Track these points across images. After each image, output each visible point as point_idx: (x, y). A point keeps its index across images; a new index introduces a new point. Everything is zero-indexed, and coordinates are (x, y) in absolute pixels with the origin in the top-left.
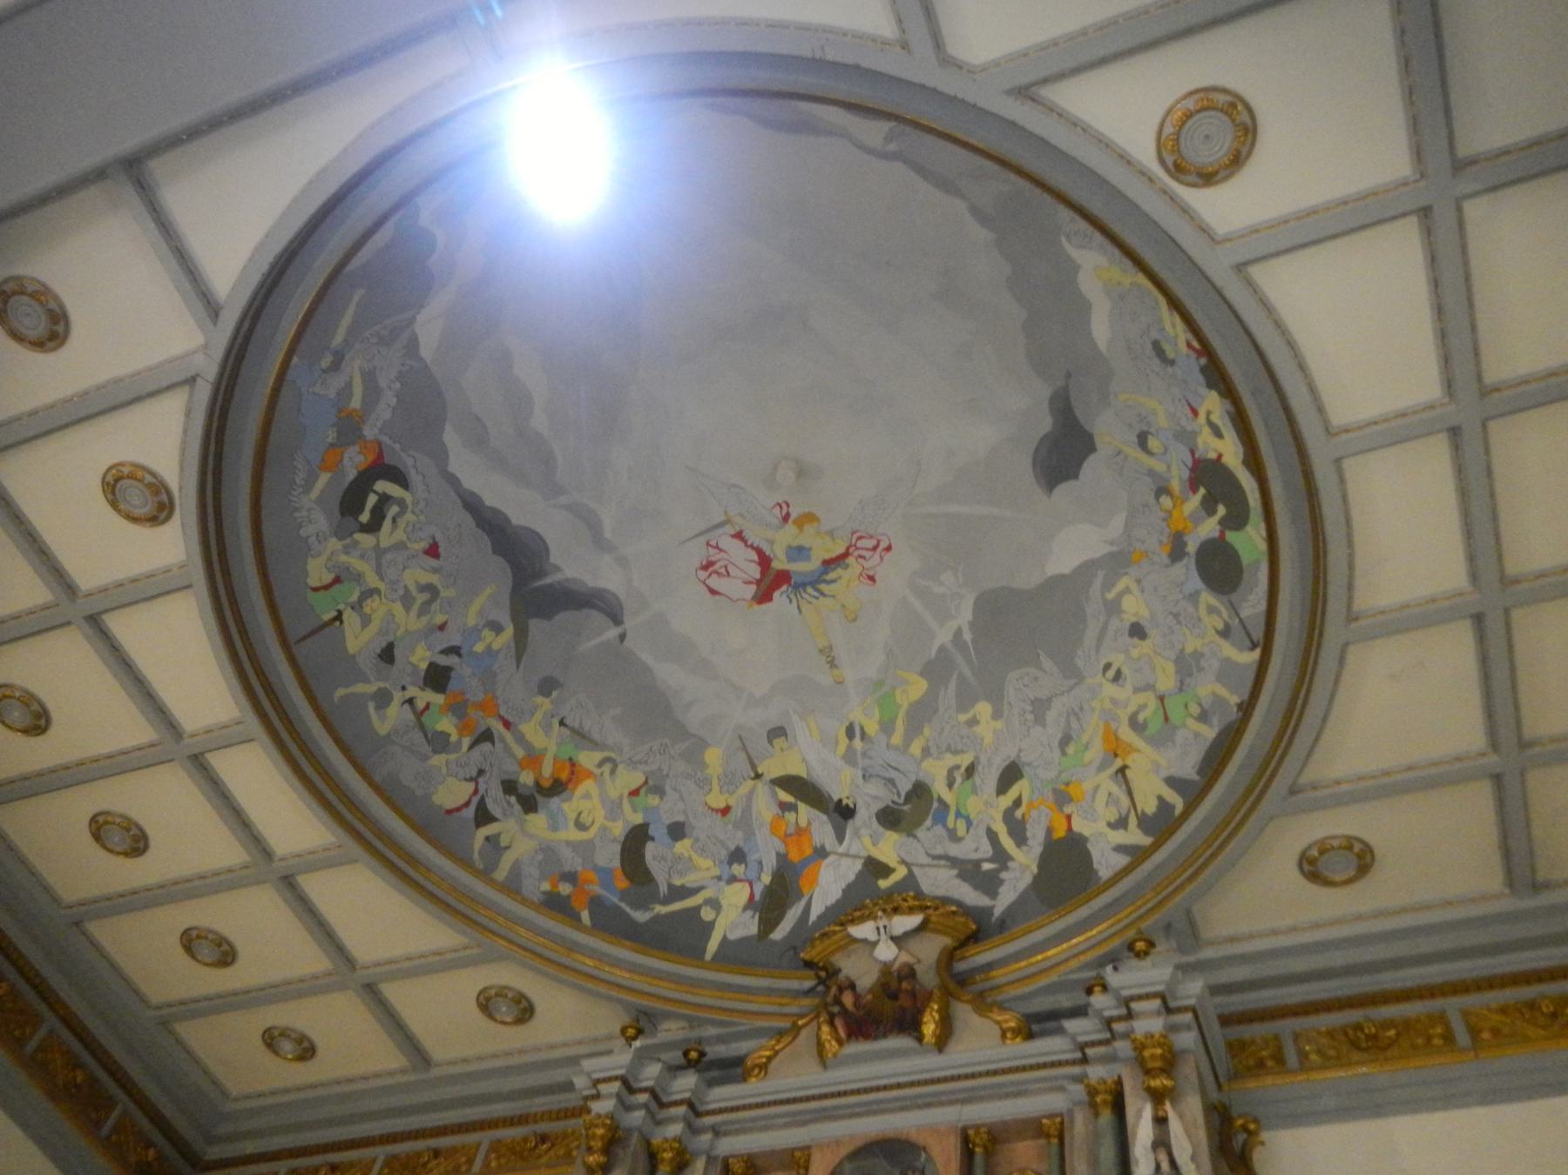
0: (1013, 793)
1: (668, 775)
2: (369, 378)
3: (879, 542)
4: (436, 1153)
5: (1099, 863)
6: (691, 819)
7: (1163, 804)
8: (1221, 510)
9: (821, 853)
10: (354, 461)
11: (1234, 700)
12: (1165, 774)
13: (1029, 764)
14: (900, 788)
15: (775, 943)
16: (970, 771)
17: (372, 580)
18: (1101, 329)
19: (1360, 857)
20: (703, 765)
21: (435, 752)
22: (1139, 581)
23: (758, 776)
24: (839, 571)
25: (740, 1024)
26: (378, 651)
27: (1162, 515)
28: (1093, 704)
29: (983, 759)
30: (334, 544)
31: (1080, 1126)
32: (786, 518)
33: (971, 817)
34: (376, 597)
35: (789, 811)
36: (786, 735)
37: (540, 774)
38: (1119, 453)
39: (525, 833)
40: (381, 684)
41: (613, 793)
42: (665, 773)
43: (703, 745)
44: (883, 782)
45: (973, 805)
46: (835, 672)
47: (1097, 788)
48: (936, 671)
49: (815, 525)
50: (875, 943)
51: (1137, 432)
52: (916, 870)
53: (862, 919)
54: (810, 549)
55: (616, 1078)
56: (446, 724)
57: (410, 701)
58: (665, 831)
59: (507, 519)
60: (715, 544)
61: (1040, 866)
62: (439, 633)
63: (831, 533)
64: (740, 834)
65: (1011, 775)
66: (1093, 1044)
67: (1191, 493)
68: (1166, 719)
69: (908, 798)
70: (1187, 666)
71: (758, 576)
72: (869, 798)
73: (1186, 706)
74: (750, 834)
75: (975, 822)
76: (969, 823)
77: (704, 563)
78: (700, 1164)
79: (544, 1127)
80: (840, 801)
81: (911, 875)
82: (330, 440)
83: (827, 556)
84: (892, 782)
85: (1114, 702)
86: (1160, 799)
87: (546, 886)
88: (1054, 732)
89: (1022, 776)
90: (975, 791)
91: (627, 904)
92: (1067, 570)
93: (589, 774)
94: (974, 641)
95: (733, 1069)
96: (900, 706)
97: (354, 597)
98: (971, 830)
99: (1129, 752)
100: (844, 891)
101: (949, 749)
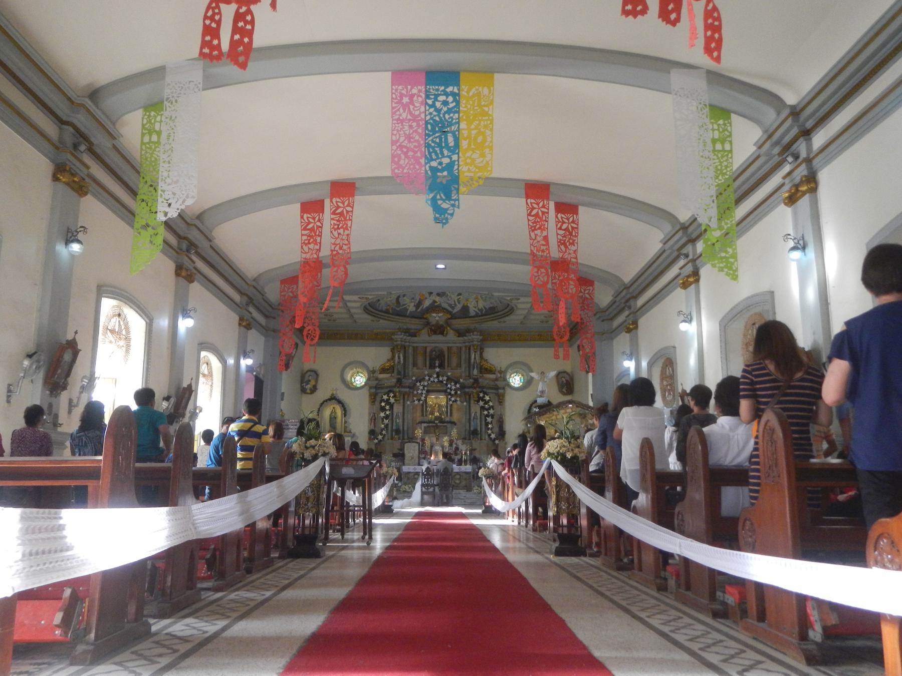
9: (426, 298)
11: (496, 305)
31: (464, 349)
45: (452, 296)
65: (459, 294)
78: (411, 348)
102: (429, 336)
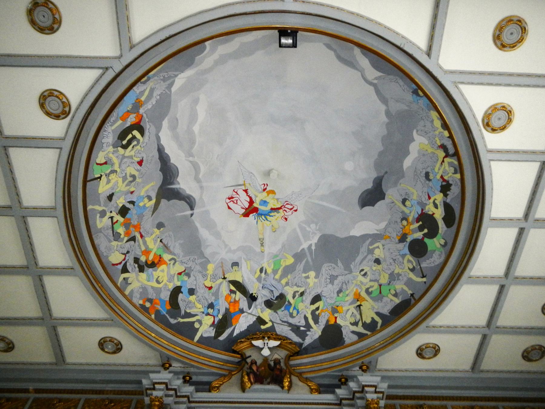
0: (316, 305)
1: (193, 270)
2: (152, 91)
3: (294, 207)
4: (60, 400)
5: (345, 336)
6: (198, 288)
7: (374, 321)
8: (426, 231)
9: (242, 311)
10: (132, 119)
11: (410, 292)
12: (375, 311)
13: (324, 297)
14: (275, 295)
15: (219, 340)
16: (302, 294)
17: (116, 167)
18: (407, 163)
19: (436, 351)
20: (207, 270)
21: (115, 240)
22: (383, 245)
23: (225, 278)
24: (275, 213)
25: (204, 369)
26: (108, 195)
27: (402, 227)
28: (353, 281)
29: (308, 291)
30: (111, 149)
32: (264, 190)
33: (299, 310)
34: (115, 174)
35: (233, 294)
36: (238, 266)
37: (148, 258)
38: (393, 203)
39: (138, 281)
40: (104, 208)
41: (172, 272)
42: (192, 269)
43: (208, 262)
44: (269, 291)
45: (301, 306)
46: (262, 248)
47: (348, 310)
48: (299, 257)
49: (274, 195)
50: (262, 349)
51: (403, 198)
52: (275, 325)
53: (257, 339)
54: (268, 203)
55: (163, 383)
56: (121, 230)
57: (112, 218)
58: (187, 290)
59: (170, 160)
60: (236, 191)
61: (322, 333)
62: (130, 194)
63: (277, 199)
64: (213, 298)
65: (317, 299)
66: (346, 399)
67: (416, 222)
68: (380, 293)
69: (277, 298)
70: (393, 277)
71: (247, 207)
72: (263, 295)
73: (390, 290)
74: (217, 299)
75: (300, 313)
76: (298, 312)
77: (230, 197)
79: (112, 396)
80: (252, 294)
81: (273, 326)
82: (128, 109)
83: (273, 207)
84: (272, 291)
85: (362, 283)
86: (372, 318)
87: (141, 302)
88: (336, 287)
89: (321, 300)
90: (302, 301)
91: (169, 315)
92: (358, 234)
93: (165, 263)
94: (315, 249)
95: (208, 387)
96: (282, 265)
97: (108, 172)
98: (299, 314)
99: (364, 301)
100: (248, 327)
101: (296, 285)
102: (243, 390)
